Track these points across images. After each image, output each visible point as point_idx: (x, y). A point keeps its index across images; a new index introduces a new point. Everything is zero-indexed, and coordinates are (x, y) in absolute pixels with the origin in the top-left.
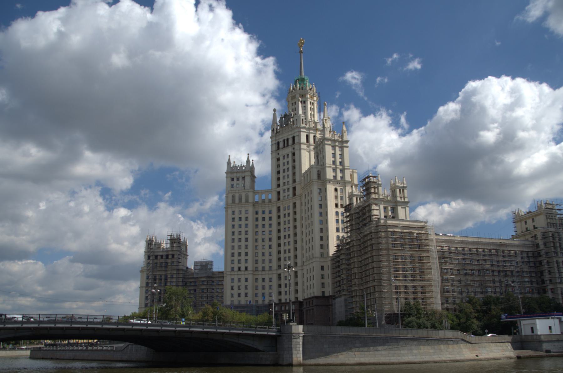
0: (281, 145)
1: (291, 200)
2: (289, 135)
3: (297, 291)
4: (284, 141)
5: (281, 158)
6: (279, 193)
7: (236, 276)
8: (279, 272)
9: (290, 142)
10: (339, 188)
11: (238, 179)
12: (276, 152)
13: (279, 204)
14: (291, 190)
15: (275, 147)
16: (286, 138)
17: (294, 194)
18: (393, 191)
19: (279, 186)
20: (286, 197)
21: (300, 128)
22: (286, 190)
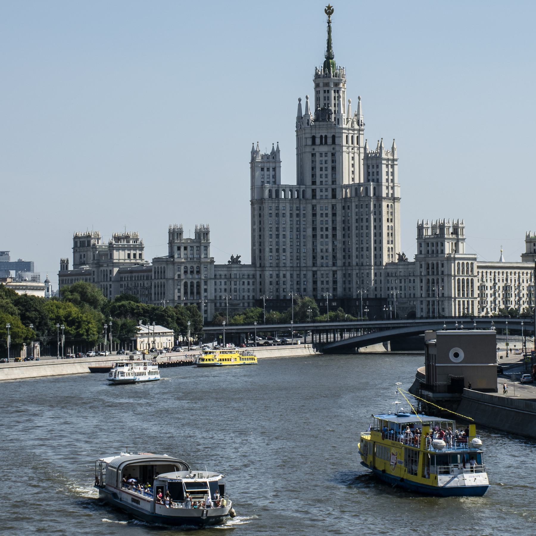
0: (318, 141)
3: (335, 289)
5: (318, 155)
6: (314, 191)
7: (274, 272)
8: (315, 269)
9: (330, 141)
10: (390, 204)
11: (268, 169)
13: (314, 201)
15: (310, 142)
16: (324, 136)
18: (455, 229)
19: (314, 183)
20: (324, 197)
21: (342, 129)
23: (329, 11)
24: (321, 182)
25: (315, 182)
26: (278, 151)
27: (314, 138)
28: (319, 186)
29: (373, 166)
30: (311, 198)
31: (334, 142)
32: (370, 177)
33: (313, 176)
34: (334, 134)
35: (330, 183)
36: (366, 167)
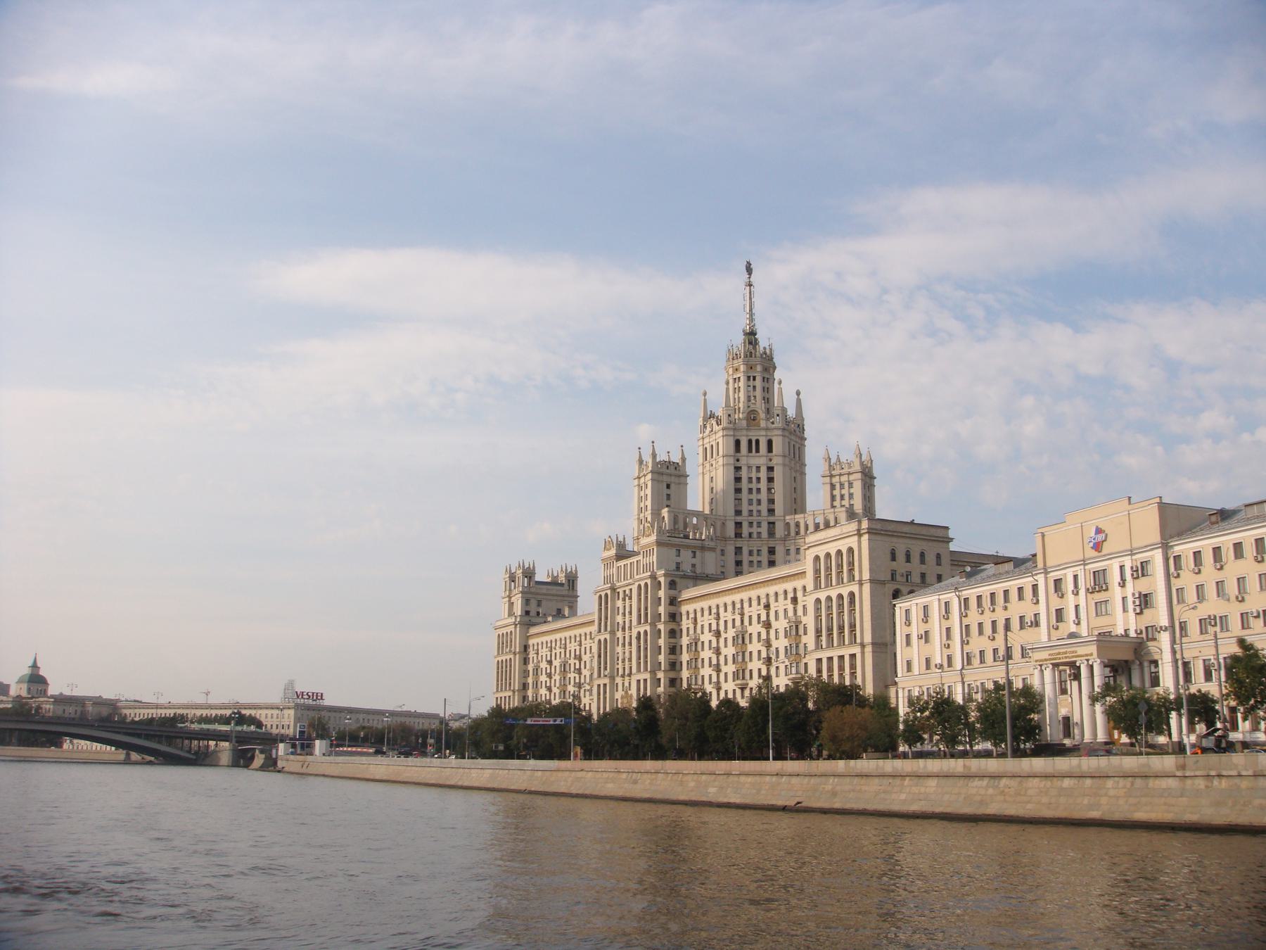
1: (766, 542)
2: (760, 436)
4: (750, 442)
5: (744, 470)
6: (738, 525)
12: (734, 456)
14: (765, 525)
17: (771, 533)
19: (738, 513)
22: (755, 524)
23: (749, 270)
24: (751, 511)
25: (741, 511)
26: (684, 459)
27: (738, 443)
28: (746, 518)
29: (842, 485)
30: (733, 535)
31: (770, 449)
32: (837, 503)
33: (738, 500)
34: (770, 438)
35: (764, 512)
36: (828, 487)
